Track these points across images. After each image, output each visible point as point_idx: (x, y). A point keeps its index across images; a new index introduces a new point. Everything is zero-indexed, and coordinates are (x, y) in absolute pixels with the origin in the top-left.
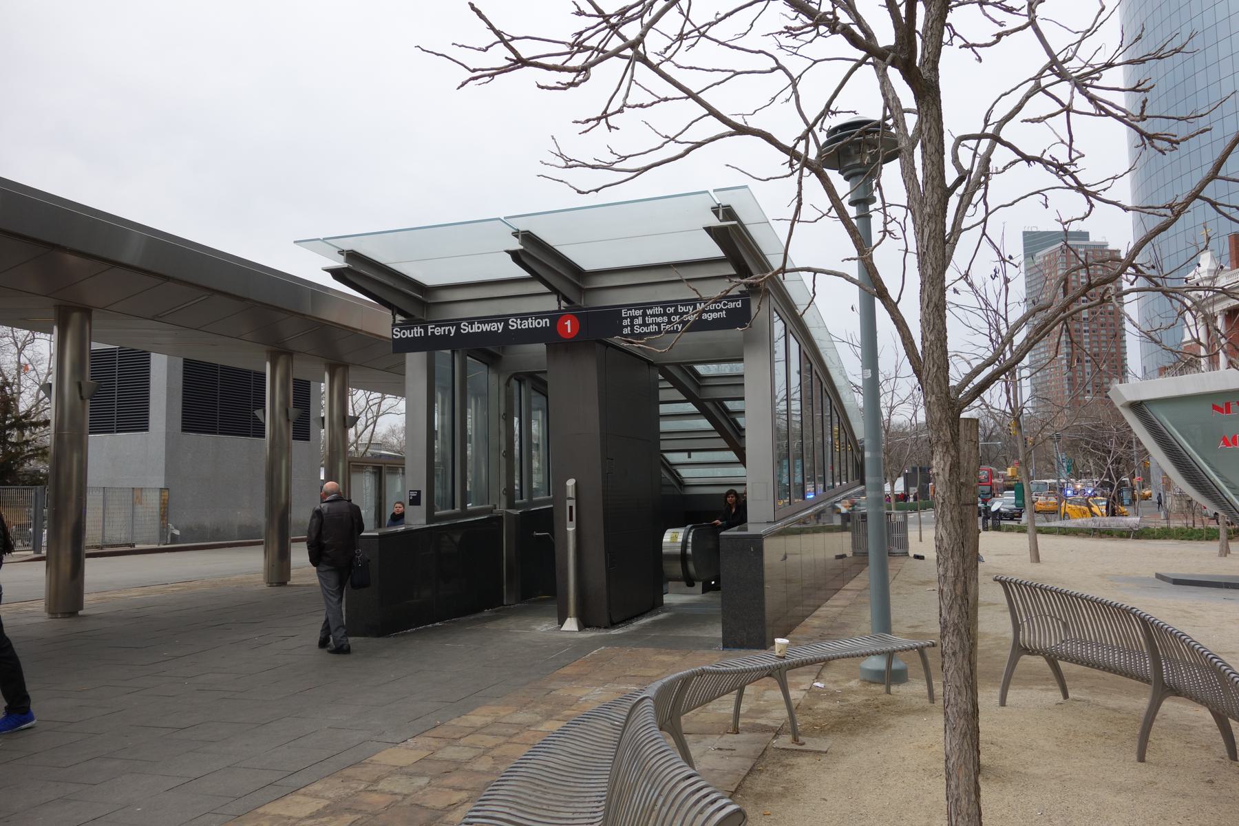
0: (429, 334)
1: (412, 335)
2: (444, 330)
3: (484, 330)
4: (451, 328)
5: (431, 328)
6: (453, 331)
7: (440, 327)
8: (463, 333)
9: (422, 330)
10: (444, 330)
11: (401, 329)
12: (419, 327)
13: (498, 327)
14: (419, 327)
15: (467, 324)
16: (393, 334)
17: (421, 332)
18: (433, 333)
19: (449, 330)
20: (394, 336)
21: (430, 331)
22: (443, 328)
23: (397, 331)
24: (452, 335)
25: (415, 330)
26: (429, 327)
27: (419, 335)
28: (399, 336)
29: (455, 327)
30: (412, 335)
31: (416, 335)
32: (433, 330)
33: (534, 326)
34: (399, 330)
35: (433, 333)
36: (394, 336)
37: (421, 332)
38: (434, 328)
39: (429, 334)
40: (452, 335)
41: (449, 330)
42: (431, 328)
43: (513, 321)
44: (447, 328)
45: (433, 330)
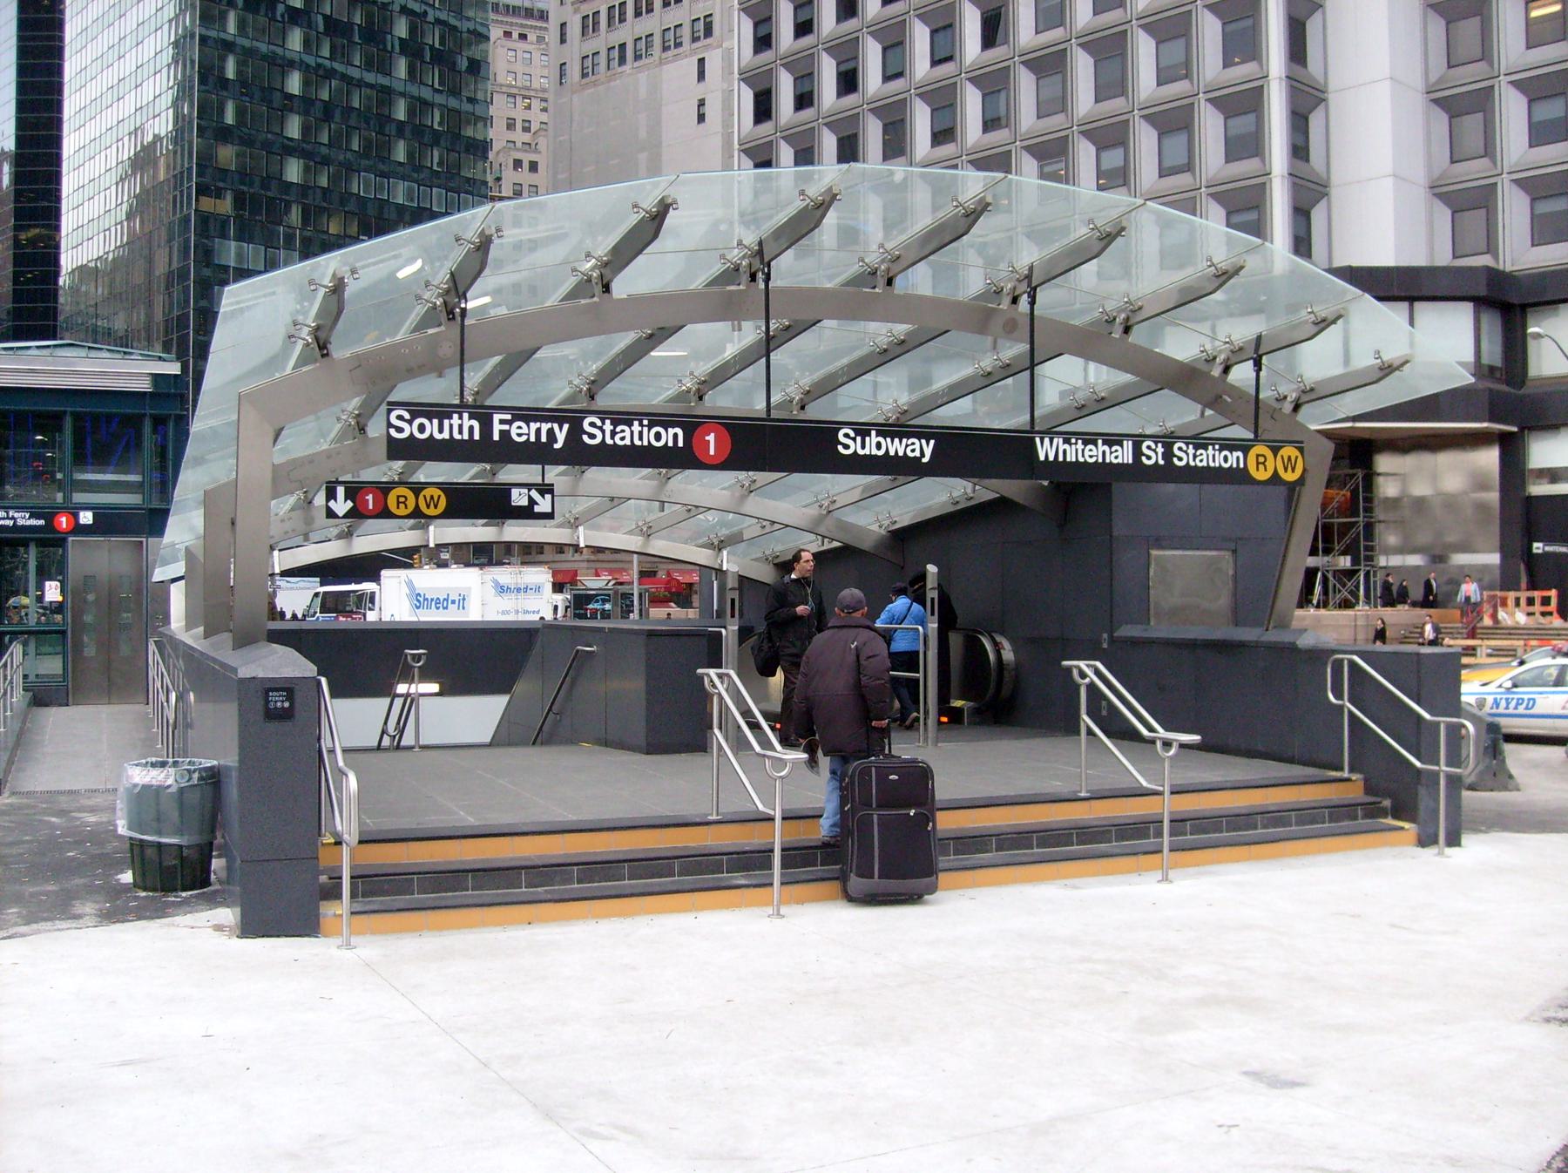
0: (496, 437)
2: (538, 431)
3: (892, 453)
4: (556, 426)
5: (502, 422)
6: (561, 436)
8: (1181, 467)
9: (476, 424)
10: (538, 431)
11: (414, 415)
12: (466, 416)
13: (1123, 455)
14: (466, 416)
15: (852, 435)
16: (390, 425)
17: (471, 428)
18: (505, 435)
19: (551, 432)
20: (393, 432)
21: (497, 428)
22: (534, 426)
23: (400, 418)
24: (558, 446)
25: (456, 420)
26: (497, 417)
27: (466, 437)
28: (598, 441)
29: (566, 427)
30: (446, 435)
31: (457, 436)
32: (506, 427)
33: (1217, 465)
34: (407, 416)
35: (505, 435)
36: (393, 432)
37: (471, 428)
38: (509, 423)
39: (496, 437)
40: (558, 446)
41: (551, 432)
42: (502, 422)
43: (592, 424)
44: (545, 427)
45: (506, 427)
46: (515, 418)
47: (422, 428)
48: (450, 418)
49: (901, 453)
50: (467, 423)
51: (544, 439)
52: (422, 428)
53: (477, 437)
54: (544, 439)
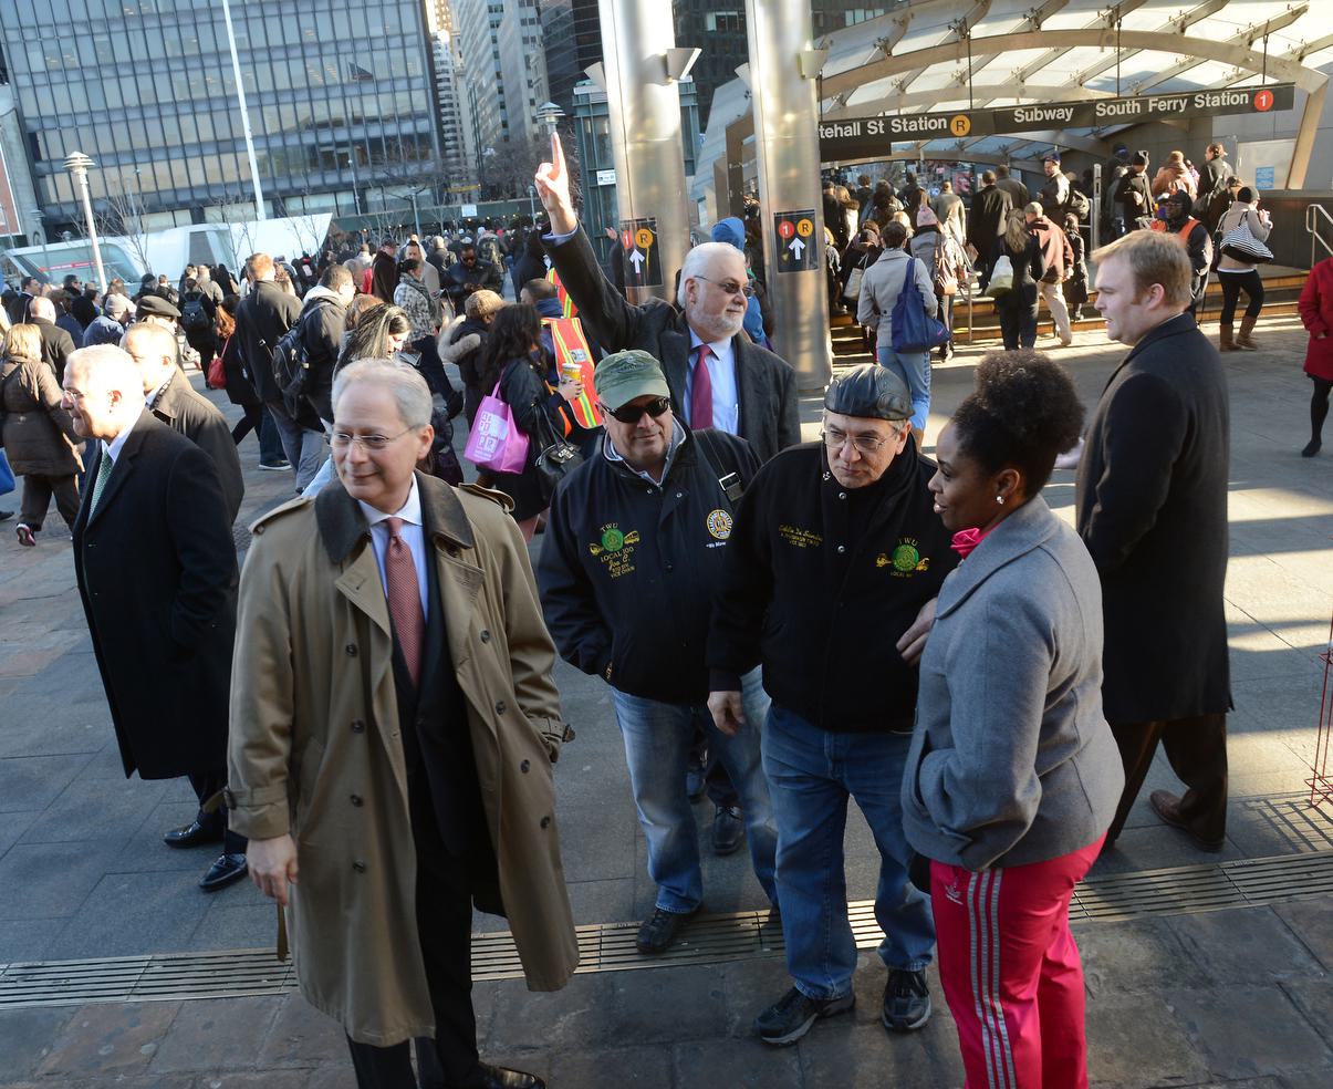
0: (1150, 110)
1: (1123, 112)
6: (1183, 106)
7: (1166, 100)
9: (1138, 105)
11: (1107, 105)
18: (1155, 109)
19: (1178, 104)
21: (1151, 105)
26: (1150, 101)
30: (1123, 112)
31: (1129, 112)
35: (1155, 109)
38: (1157, 102)
39: (1150, 110)
41: (1178, 104)
46: (1160, 100)
48: (1125, 103)
49: (1053, 118)
50: (1134, 105)
51: (1174, 108)
53: (1139, 111)
54: (1174, 108)
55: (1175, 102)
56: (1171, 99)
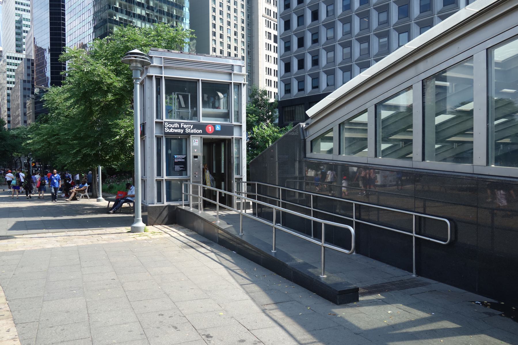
0: (181, 127)
7: (186, 124)
9: (178, 125)
11: (169, 124)
18: (183, 127)
22: (187, 125)
25: (175, 124)
26: (181, 124)
31: (175, 127)
35: (183, 127)
39: (181, 127)
41: (190, 126)
46: (184, 124)
47: (170, 125)
50: (177, 125)
52: (170, 125)
53: (178, 127)
55: (189, 126)
56: (188, 124)
